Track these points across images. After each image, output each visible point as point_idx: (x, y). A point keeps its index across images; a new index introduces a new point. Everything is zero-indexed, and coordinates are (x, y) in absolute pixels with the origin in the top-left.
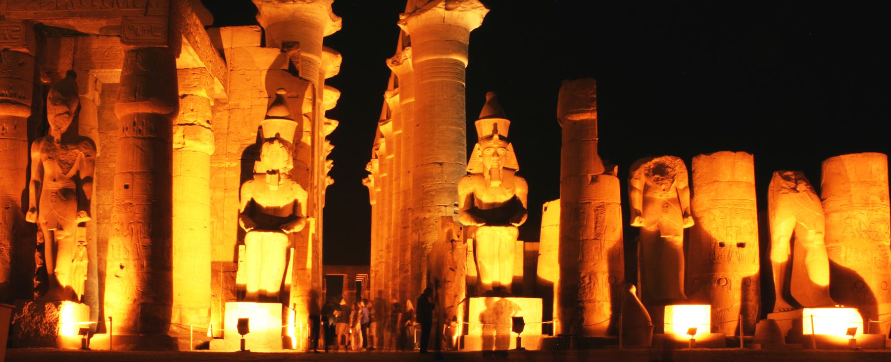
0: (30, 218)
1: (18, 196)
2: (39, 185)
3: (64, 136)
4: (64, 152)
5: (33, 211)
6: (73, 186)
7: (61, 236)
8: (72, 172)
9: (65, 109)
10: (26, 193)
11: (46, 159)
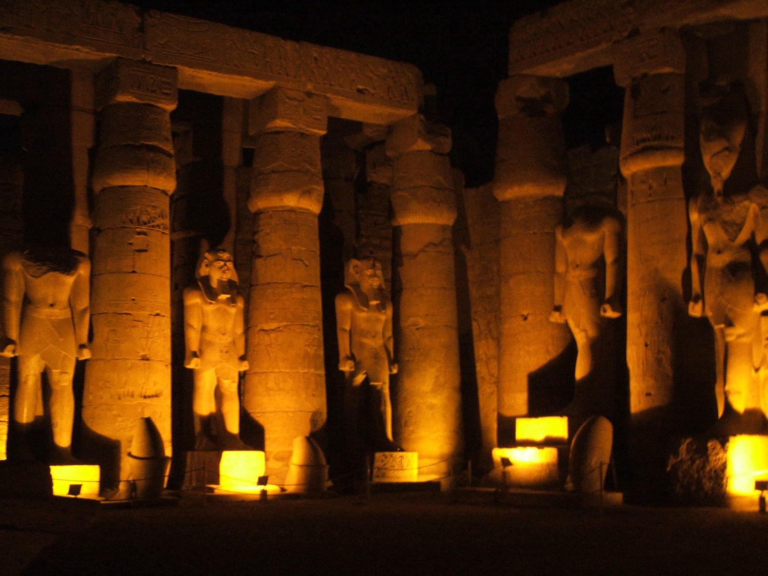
0: (695, 310)
1: (675, 279)
2: (702, 261)
3: (727, 184)
4: (728, 208)
5: (696, 301)
6: (746, 257)
7: (733, 335)
8: (743, 236)
9: (724, 143)
10: (687, 274)
11: (705, 222)
